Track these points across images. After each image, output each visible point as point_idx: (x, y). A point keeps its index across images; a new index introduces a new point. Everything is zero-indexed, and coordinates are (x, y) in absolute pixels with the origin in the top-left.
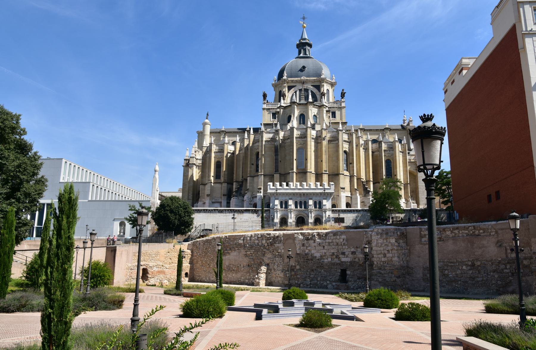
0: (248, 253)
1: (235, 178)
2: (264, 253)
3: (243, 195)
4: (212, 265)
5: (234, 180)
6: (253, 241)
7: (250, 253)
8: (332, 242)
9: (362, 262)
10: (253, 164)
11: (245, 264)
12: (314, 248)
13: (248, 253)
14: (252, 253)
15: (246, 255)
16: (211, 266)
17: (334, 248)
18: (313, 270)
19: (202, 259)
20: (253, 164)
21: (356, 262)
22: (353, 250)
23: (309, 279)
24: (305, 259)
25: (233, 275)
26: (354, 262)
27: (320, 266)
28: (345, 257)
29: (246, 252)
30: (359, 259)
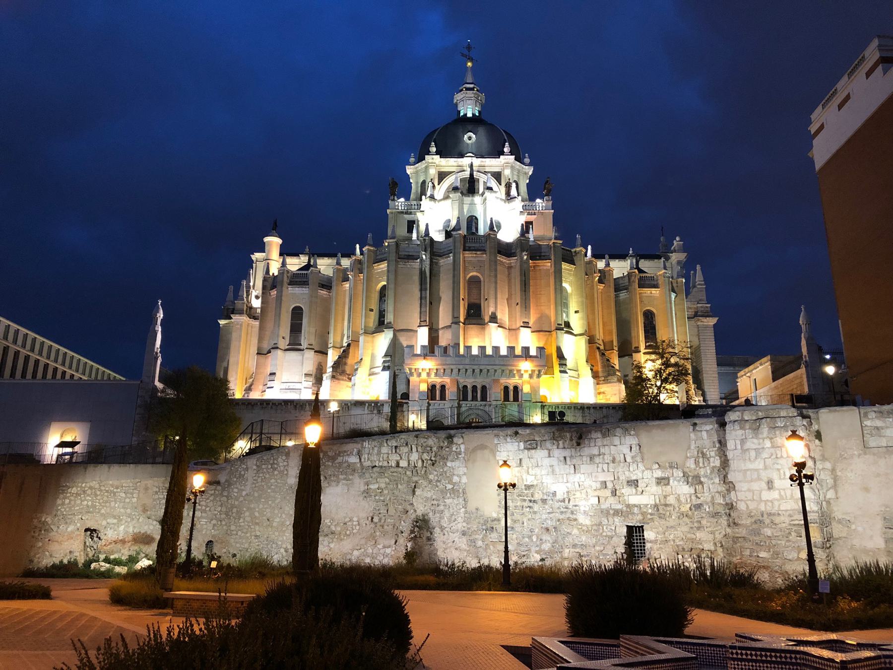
0: (372, 487)
1: (331, 340)
2: (414, 485)
3: (349, 375)
4: (277, 520)
5: (330, 346)
6: (385, 456)
7: (376, 486)
8: (599, 455)
9: (689, 506)
10: (371, 310)
11: (363, 515)
12: (550, 470)
13: (372, 487)
14: (383, 486)
15: (367, 493)
16: (275, 524)
17: (606, 469)
18: (547, 530)
19: (252, 506)
20: (371, 310)
21: (671, 505)
22: (659, 474)
23: (537, 552)
24: (525, 500)
25: (332, 545)
26: (666, 505)
27: (568, 519)
28: (636, 494)
29: (367, 484)
30: (678, 500)
